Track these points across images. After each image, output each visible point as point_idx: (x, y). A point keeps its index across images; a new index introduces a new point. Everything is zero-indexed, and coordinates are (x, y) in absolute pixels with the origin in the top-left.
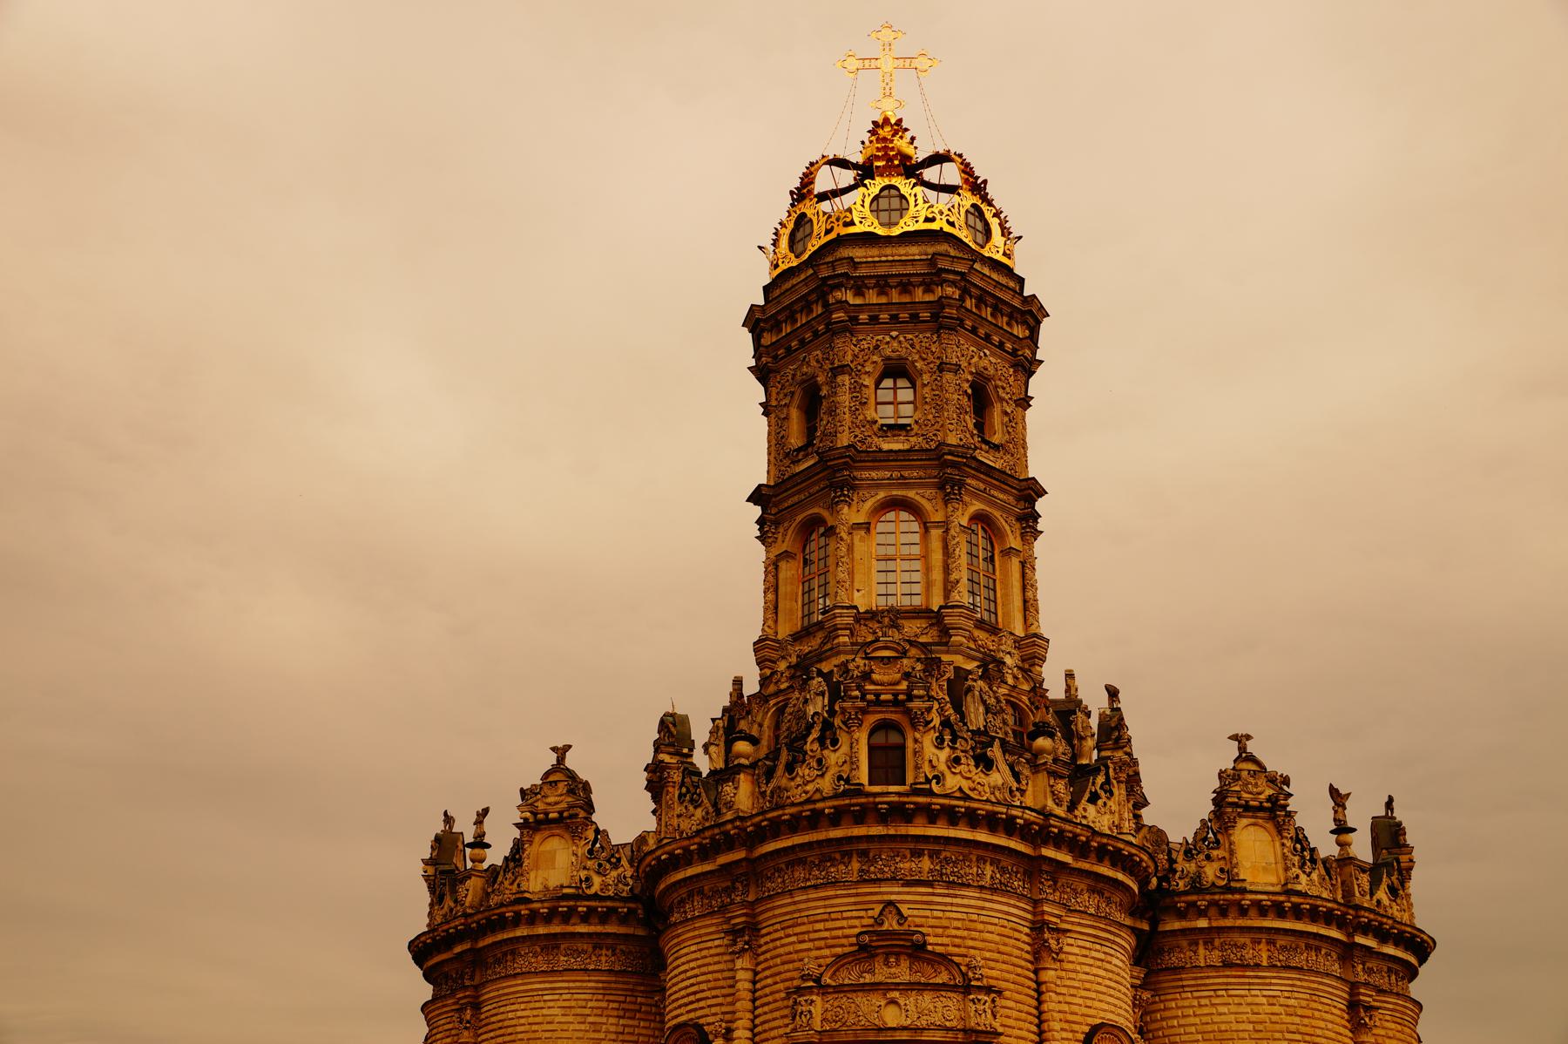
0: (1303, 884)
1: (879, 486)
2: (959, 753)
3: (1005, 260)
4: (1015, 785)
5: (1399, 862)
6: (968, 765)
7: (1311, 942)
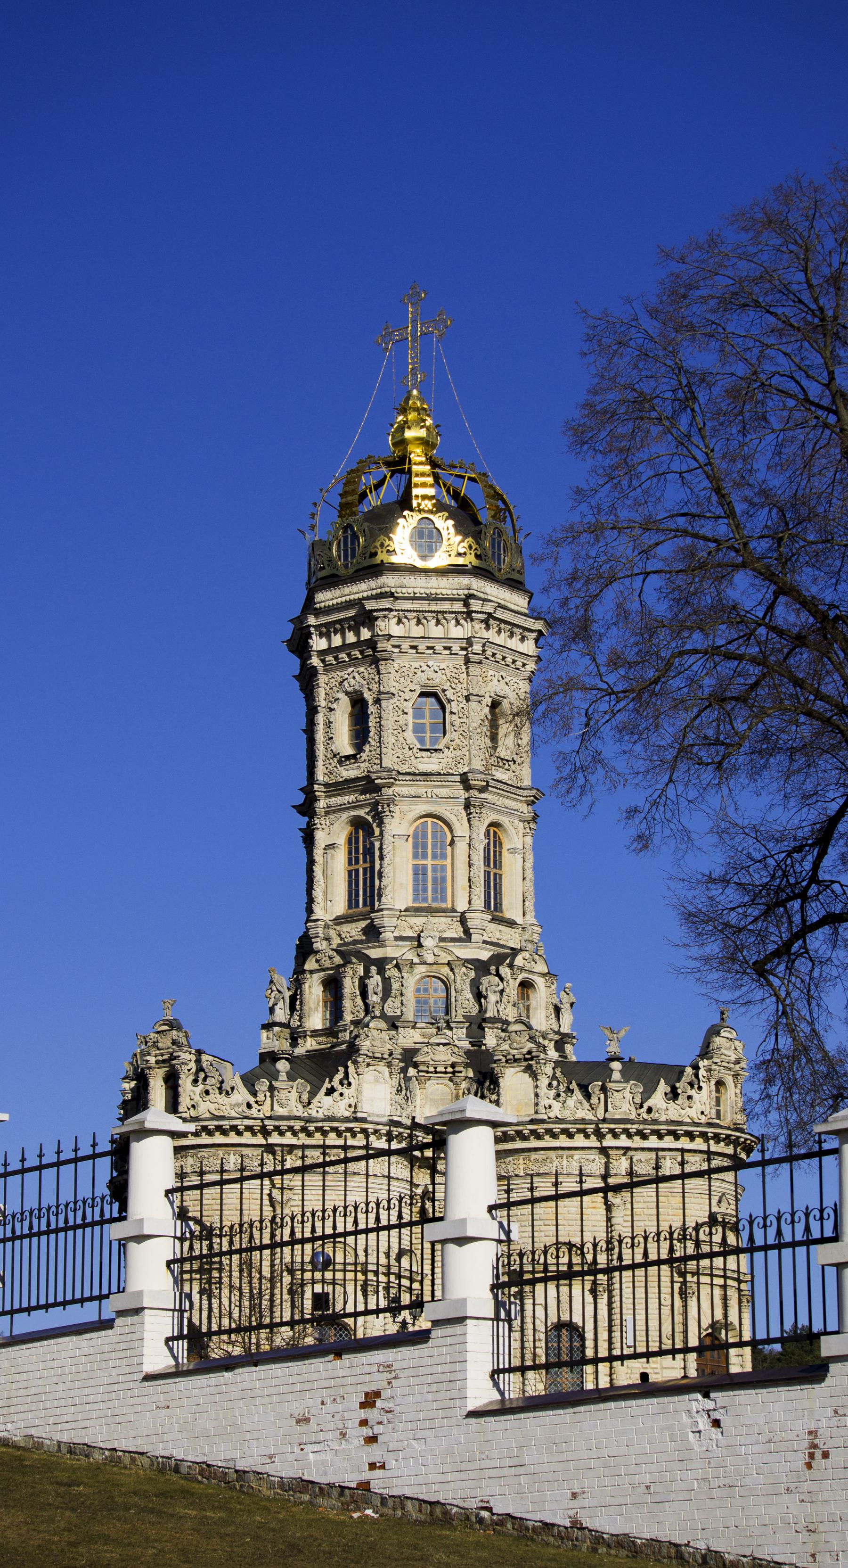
0: (556, 1111)
1: (341, 810)
2: (208, 1088)
3: (461, 561)
4: (252, 1100)
5: (696, 1068)
6: (215, 1095)
7: (560, 1152)
